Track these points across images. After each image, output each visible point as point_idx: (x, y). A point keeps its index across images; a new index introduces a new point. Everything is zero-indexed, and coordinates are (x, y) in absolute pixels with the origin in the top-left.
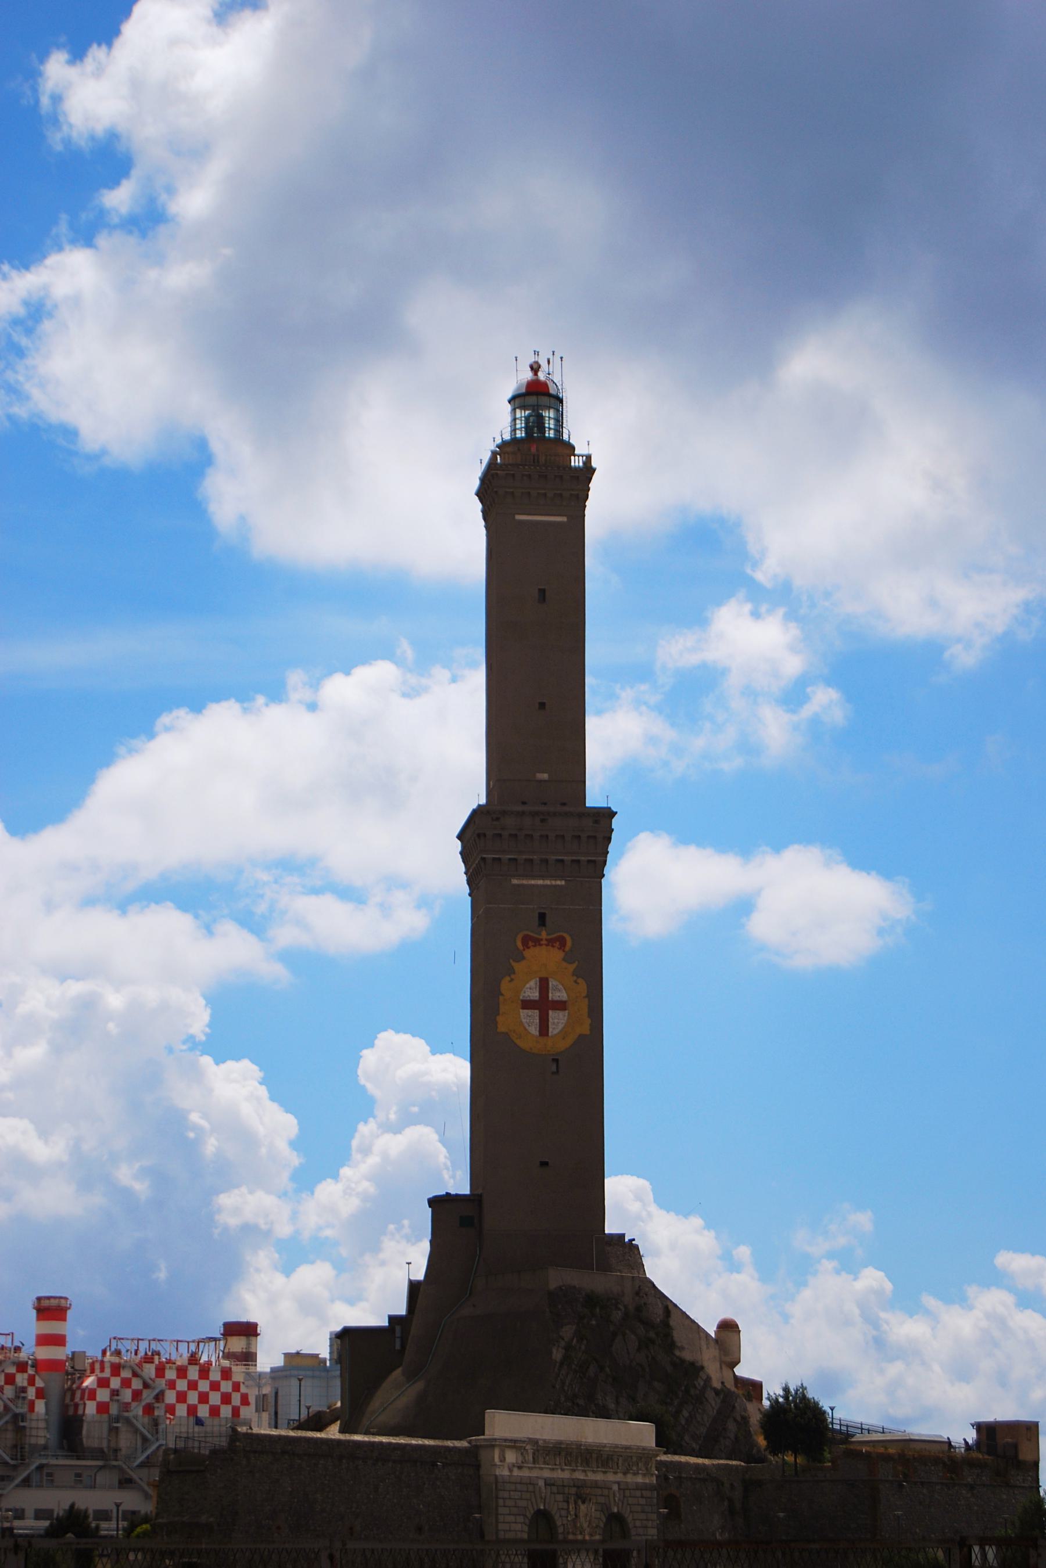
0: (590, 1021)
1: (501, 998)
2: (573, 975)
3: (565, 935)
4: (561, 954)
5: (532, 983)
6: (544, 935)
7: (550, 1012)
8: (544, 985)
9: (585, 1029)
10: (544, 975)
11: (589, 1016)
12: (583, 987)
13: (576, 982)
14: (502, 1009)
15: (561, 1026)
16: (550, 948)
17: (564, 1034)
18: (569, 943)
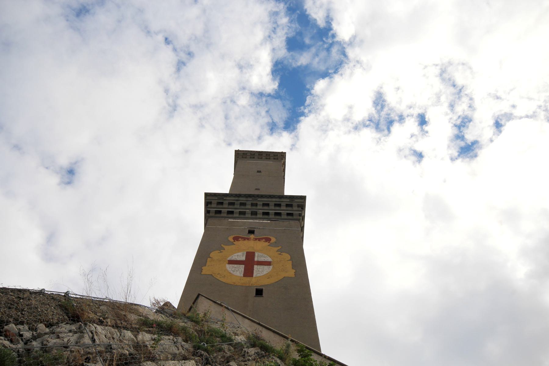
0: (294, 271)
1: (209, 259)
2: (277, 251)
3: (271, 237)
4: (267, 244)
5: (240, 254)
6: (252, 236)
7: (255, 267)
8: (250, 256)
9: (291, 273)
10: (250, 250)
11: (293, 268)
12: (287, 256)
13: (280, 254)
14: (208, 263)
15: (265, 273)
16: (257, 241)
17: (268, 276)
18: (273, 240)
